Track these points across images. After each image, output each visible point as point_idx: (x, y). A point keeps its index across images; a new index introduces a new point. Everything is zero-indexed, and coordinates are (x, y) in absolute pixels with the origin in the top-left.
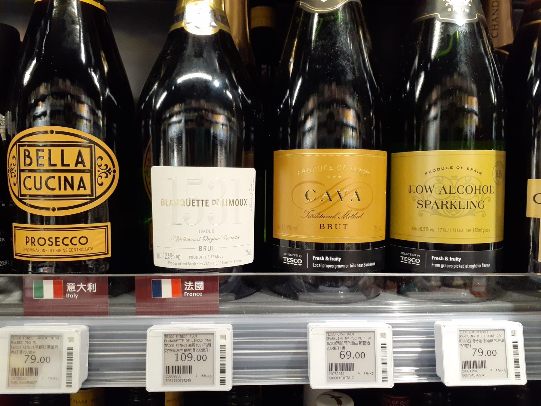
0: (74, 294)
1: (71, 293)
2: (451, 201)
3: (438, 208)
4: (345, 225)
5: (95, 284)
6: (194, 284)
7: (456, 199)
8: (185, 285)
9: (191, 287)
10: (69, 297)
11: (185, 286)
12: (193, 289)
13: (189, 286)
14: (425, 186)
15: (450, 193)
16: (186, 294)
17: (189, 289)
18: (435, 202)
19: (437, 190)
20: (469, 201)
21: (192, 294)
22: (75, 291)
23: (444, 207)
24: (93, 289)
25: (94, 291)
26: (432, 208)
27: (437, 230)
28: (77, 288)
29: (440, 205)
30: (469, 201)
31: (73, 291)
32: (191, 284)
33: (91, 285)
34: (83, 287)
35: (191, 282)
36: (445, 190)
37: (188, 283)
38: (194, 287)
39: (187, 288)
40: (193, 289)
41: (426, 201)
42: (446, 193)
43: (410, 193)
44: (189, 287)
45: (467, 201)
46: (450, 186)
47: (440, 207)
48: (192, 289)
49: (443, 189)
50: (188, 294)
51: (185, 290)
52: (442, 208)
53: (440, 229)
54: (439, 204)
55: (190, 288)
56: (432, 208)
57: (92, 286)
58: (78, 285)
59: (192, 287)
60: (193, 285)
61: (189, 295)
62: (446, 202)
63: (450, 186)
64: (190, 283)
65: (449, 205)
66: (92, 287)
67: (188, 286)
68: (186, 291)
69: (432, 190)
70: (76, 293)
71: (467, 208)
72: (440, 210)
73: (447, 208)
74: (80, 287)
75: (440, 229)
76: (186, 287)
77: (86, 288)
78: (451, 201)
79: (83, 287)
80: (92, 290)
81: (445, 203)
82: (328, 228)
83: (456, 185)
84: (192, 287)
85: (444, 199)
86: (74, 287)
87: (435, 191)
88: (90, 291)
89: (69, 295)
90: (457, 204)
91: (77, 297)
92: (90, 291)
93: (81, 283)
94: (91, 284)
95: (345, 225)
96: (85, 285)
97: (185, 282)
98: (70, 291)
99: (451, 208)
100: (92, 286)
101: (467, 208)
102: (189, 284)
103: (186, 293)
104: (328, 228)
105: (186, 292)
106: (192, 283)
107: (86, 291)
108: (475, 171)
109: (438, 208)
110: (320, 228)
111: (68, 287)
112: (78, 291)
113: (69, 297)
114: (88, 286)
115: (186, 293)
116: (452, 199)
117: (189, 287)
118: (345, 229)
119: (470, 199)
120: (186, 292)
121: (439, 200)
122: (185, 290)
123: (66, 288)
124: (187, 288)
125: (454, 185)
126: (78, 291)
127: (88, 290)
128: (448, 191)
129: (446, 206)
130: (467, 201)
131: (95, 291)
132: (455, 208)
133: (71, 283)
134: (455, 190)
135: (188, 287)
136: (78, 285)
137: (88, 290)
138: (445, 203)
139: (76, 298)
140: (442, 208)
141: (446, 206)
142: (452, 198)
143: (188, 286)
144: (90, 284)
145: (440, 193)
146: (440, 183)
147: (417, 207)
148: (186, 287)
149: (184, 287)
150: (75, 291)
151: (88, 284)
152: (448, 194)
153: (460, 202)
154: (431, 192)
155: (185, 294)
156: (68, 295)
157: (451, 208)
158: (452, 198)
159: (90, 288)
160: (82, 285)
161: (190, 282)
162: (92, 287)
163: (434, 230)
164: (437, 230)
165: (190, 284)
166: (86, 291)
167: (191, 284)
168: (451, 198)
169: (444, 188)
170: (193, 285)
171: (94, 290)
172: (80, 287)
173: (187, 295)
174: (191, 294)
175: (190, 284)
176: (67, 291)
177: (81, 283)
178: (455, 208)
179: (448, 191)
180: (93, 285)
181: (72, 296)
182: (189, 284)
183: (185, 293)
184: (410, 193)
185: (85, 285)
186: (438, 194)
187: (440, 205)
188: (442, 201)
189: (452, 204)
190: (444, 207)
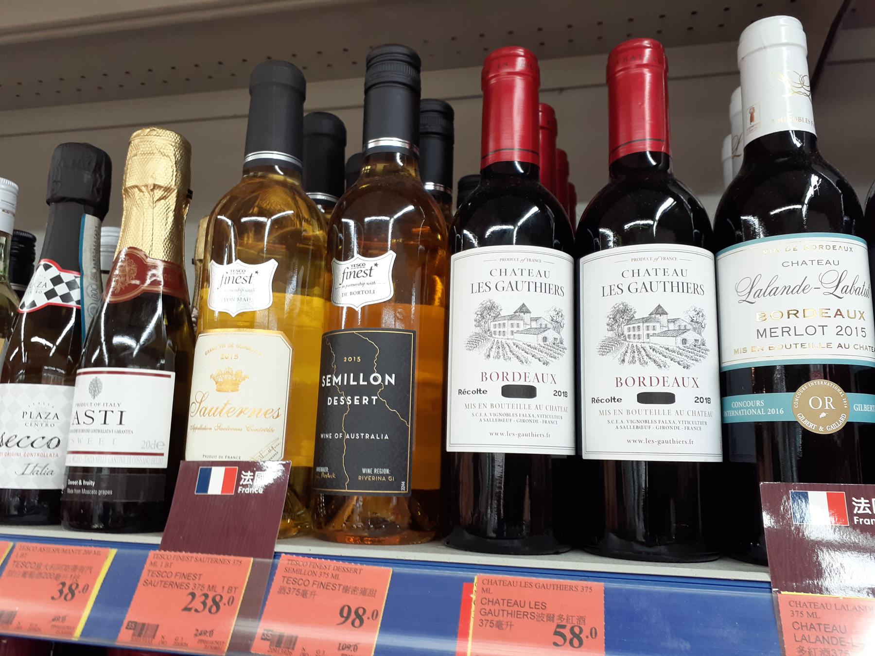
5: (675, 203)
6: (870, 503)
8: (854, 503)
9: (865, 507)
11: (855, 506)
12: (870, 513)
13: (862, 506)
16: (858, 520)
17: (861, 511)
21: (868, 520)
32: (865, 503)
35: (865, 499)
37: (859, 501)
38: (871, 508)
39: (858, 510)
40: (870, 513)
44: (862, 509)
48: (868, 511)
50: (861, 520)
51: (855, 512)
55: (864, 509)
59: (866, 508)
60: (869, 505)
61: (863, 521)
64: (863, 500)
67: (859, 505)
68: (857, 515)
76: (857, 508)
84: (866, 508)
97: (854, 499)
102: (860, 503)
103: (857, 519)
105: (858, 518)
106: (868, 501)
115: (857, 519)
117: (862, 509)
120: (858, 518)
122: (855, 512)
124: (858, 510)
135: (859, 508)
143: (859, 505)
148: (857, 508)
149: (851, 508)
155: (856, 521)
161: (862, 498)
165: (863, 503)
167: (865, 503)
170: (869, 505)
173: (859, 522)
174: (867, 522)
175: (863, 503)
182: (860, 503)
183: (855, 518)
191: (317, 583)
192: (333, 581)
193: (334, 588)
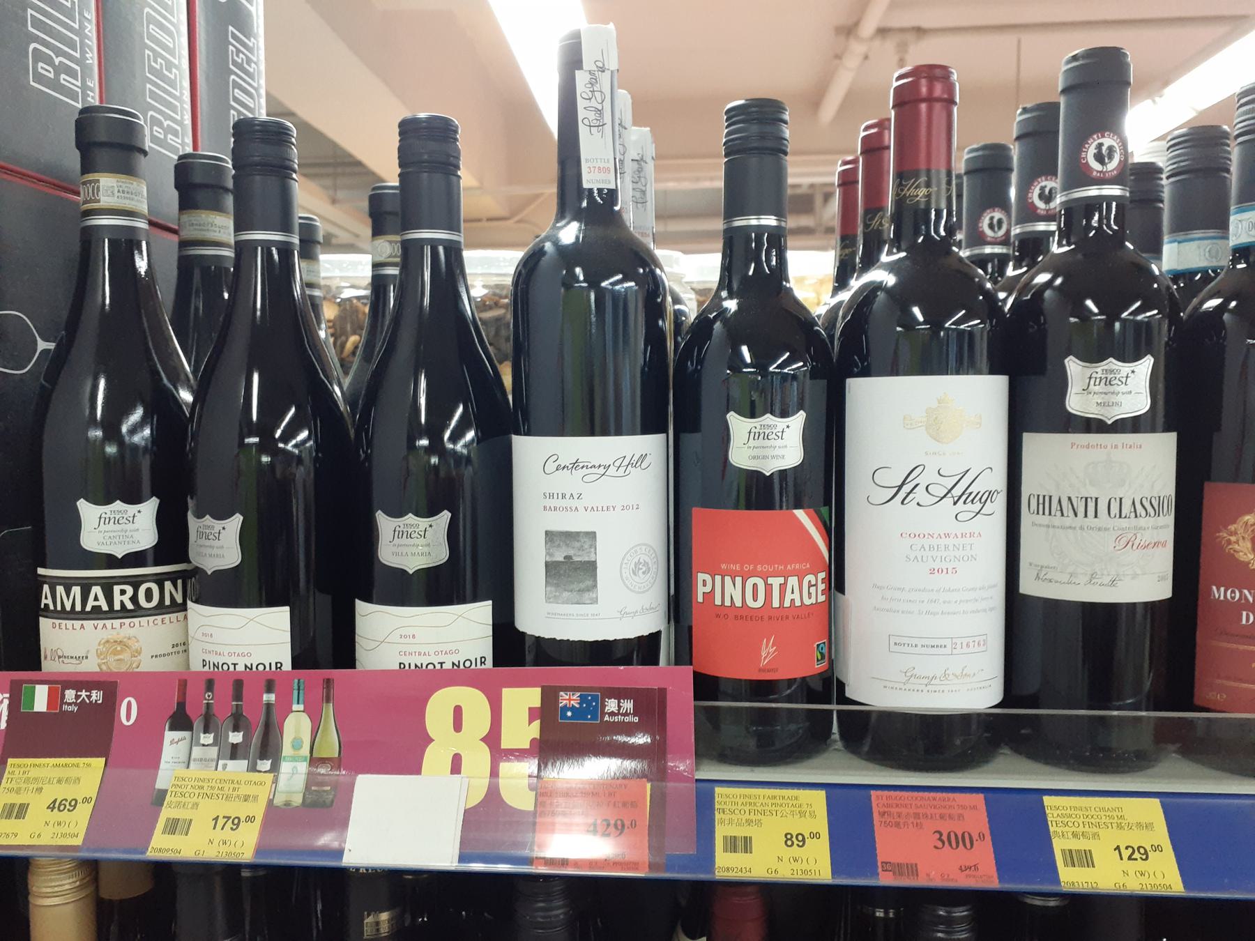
1: (70, 704)
5: (102, 692)
25: (99, 702)
28: (77, 697)
33: (97, 693)
34: (86, 695)
58: (79, 693)
70: (75, 704)
74: (81, 695)
77: (89, 697)
79: (86, 695)
80: (96, 701)
86: (74, 696)
88: (94, 701)
91: (76, 709)
93: (84, 691)
96: (88, 693)
98: (68, 701)
107: (88, 701)
111: (66, 696)
112: (78, 701)
123: (63, 696)
126: (78, 701)
136: (79, 693)
144: (94, 692)
156: (65, 707)
159: (94, 698)
160: (84, 694)
166: (88, 701)
172: (81, 695)
177: (84, 691)
181: (70, 708)
185: (88, 693)
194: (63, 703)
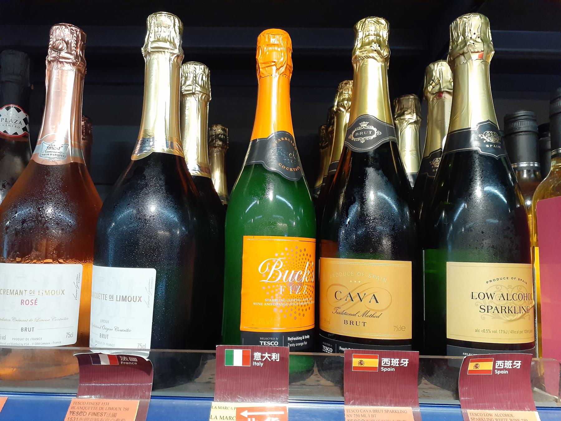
0: (260, 362)
1: (257, 361)
2: (509, 307)
3: (498, 312)
4: (364, 322)
5: (279, 354)
7: (512, 305)
10: (255, 365)
14: (487, 294)
15: (507, 300)
18: (496, 307)
19: (497, 297)
20: (521, 307)
22: (261, 360)
23: (503, 311)
24: (277, 359)
25: (277, 360)
26: (493, 312)
27: (498, 331)
28: (262, 357)
29: (500, 310)
30: (521, 307)
31: (259, 360)
34: (268, 356)
36: (503, 297)
41: (488, 306)
42: (504, 300)
43: (472, 298)
45: (520, 307)
46: (507, 294)
47: (500, 312)
49: (502, 296)
52: (502, 313)
53: (501, 331)
54: (499, 308)
56: (493, 312)
57: (275, 356)
58: (263, 355)
62: (505, 308)
63: (507, 294)
65: (507, 310)
66: (276, 357)
69: (493, 297)
70: (262, 361)
71: (520, 313)
72: (500, 314)
73: (506, 313)
74: (265, 356)
75: (501, 331)
77: (270, 357)
78: (509, 307)
79: (268, 356)
81: (504, 308)
82: (350, 324)
83: (511, 293)
85: (503, 305)
86: (260, 357)
87: (496, 297)
88: (274, 360)
89: (255, 363)
90: (512, 309)
91: (262, 365)
92: (274, 360)
93: (267, 353)
94: (275, 354)
95: (364, 322)
96: (270, 355)
98: (256, 360)
99: (509, 313)
100: (275, 356)
101: (520, 313)
104: (350, 324)
107: (270, 360)
108: (523, 281)
109: (498, 312)
110: (345, 324)
112: (263, 360)
113: (255, 365)
114: (272, 356)
116: (509, 305)
118: (364, 326)
119: (521, 305)
121: (499, 305)
123: (253, 357)
125: (510, 293)
126: (263, 360)
127: (272, 359)
128: (506, 298)
129: (505, 311)
130: (520, 307)
131: (278, 360)
132: (512, 313)
133: (258, 353)
134: (511, 298)
136: (263, 355)
137: (272, 359)
138: (504, 308)
139: (262, 366)
140: (502, 313)
141: (505, 311)
142: (509, 304)
145: (500, 300)
146: (499, 291)
147: (480, 311)
150: (261, 360)
151: (272, 354)
152: (506, 301)
153: (515, 307)
154: (492, 299)
157: (509, 313)
158: (509, 304)
160: (267, 355)
162: (276, 357)
163: (495, 332)
164: (498, 331)
166: (270, 360)
168: (507, 305)
169: (503, 295)
171: (278, 359)
172: (265, 356)
176: (254, 360)
178: (512, 313)
179: (506, 298)
180: (277, 354)
181: (258, 364)
184: (472, 298)
185: (270, 355)
186: (497, 300)
187: (500, 310)
188: (501, 307)
189: (509, 309)
190: (503, 311)
191: (91, 413)
192: (101, 411)
193: (101, 415)
194: (253, 360)
